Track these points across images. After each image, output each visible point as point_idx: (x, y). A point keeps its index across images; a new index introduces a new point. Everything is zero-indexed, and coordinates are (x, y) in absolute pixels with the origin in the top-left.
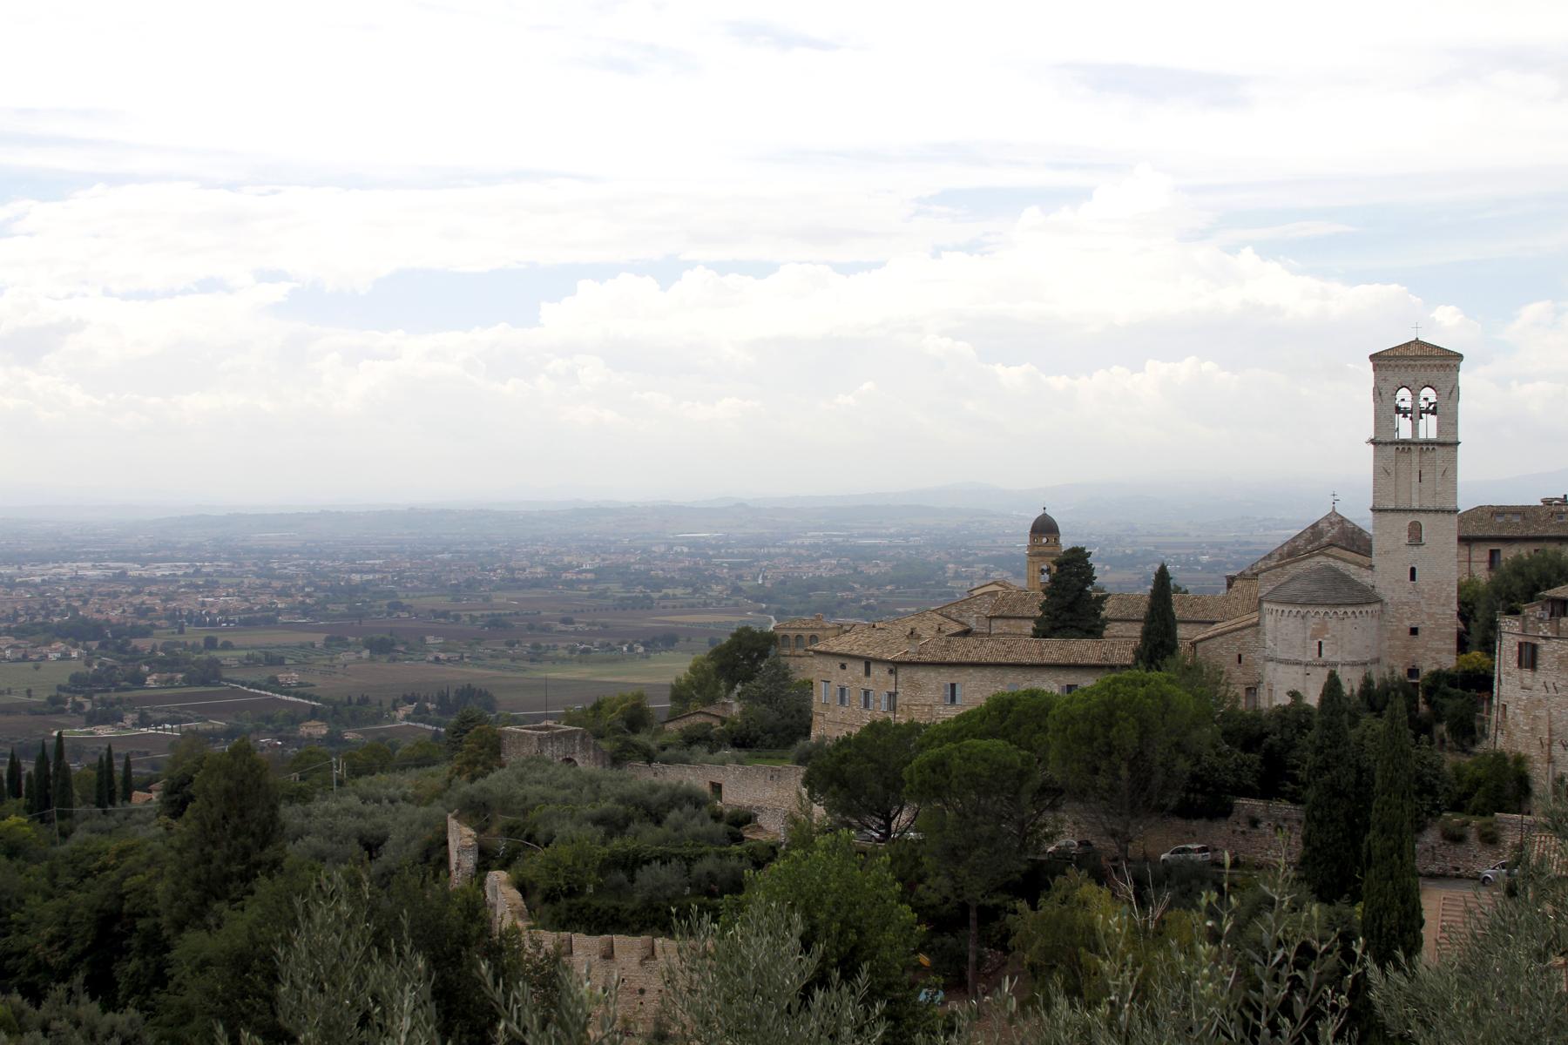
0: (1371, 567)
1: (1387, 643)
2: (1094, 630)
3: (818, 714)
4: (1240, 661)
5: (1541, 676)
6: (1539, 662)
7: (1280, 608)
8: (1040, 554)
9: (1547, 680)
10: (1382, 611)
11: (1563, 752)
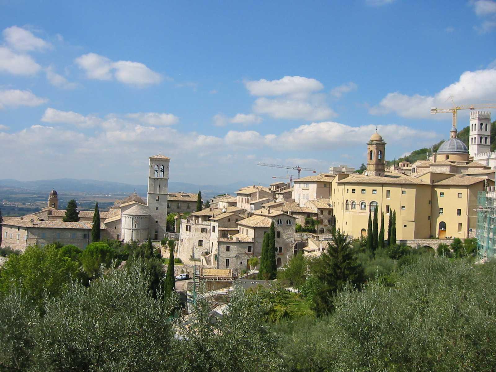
2: (77, 219)
3: (3, 241)
5: (191, 233)
7: (127, 216)
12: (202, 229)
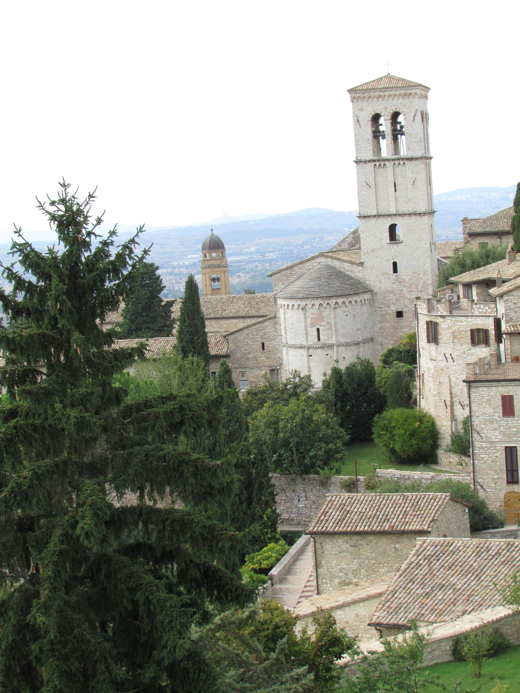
0: (361, 264)
1: (379, 325)
4: (263, 348)
6: (440, 337)
8: (209, 267)
9: (446, 352)
10: (373, 299)
11: (461, 411)
12: (472, 331)
